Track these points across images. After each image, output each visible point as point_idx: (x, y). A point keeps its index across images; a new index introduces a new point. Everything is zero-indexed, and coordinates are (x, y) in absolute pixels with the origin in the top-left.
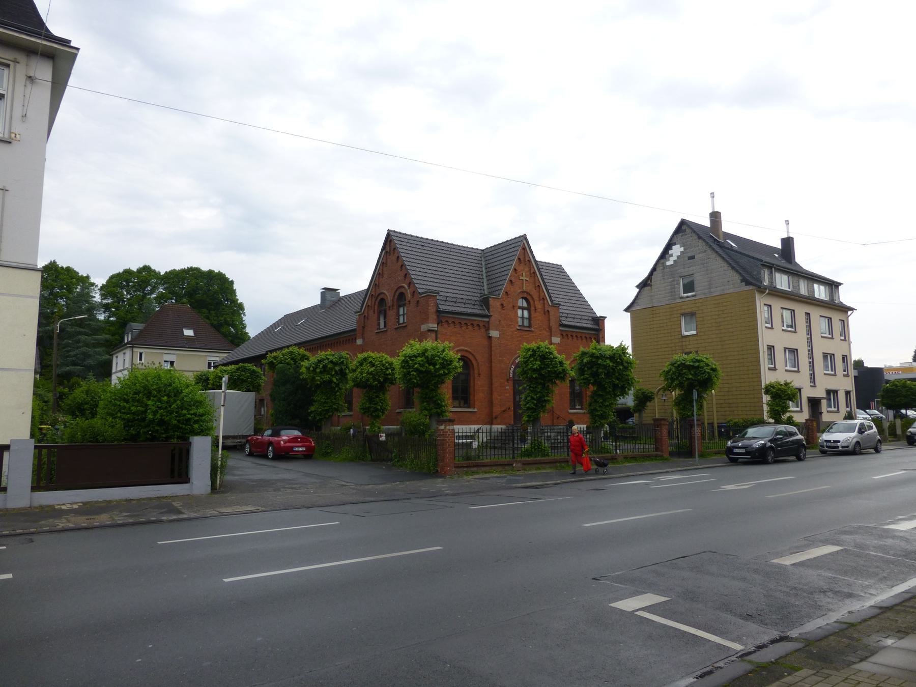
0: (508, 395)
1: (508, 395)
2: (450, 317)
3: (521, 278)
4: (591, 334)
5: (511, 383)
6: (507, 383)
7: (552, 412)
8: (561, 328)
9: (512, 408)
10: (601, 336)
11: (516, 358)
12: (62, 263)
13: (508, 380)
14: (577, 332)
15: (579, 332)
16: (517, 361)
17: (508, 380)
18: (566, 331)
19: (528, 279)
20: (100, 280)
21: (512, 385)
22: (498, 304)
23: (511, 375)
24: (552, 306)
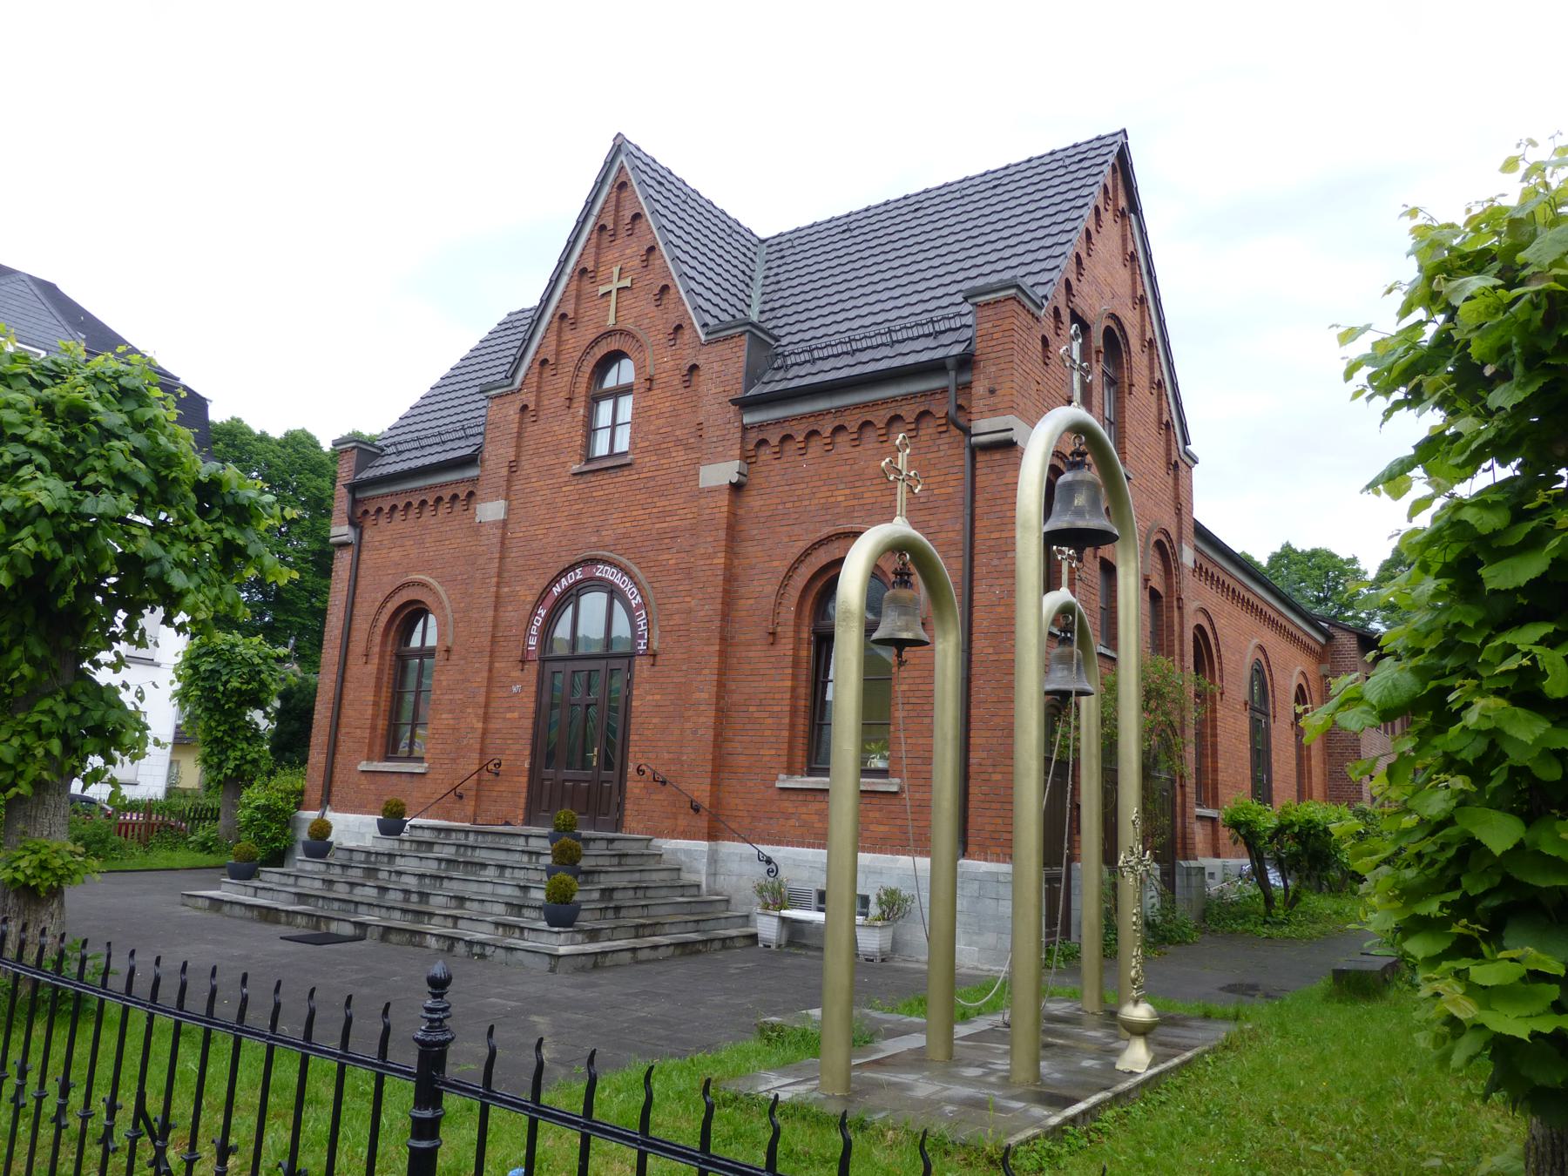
0: (516, 715)
1: (516, 715)
2: (383, 496)
3: (603, 290)
4: (924, 394)
5: (532, 669)
6: (516, 674)
7: (700, 790)
8: (748, 419)
9: (527, 765)
10: (980, 388)
11: (556, 580)
12: (1303, 544)
13: (523, 662)
14: (840, 411)
15: (847, 408)
16: (557, 590)
17: (523, 662)
18: (778, 422)
19: (627, 282)
20: (1371, 566)
21: (533, 678)
22: (512, 411)
23: (533, 641)
24: (709, 343)
